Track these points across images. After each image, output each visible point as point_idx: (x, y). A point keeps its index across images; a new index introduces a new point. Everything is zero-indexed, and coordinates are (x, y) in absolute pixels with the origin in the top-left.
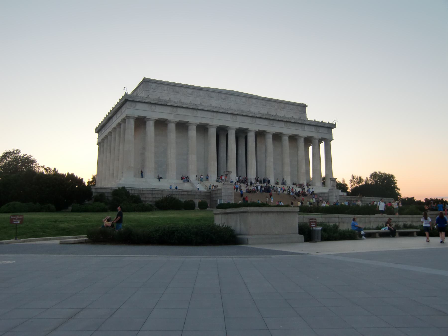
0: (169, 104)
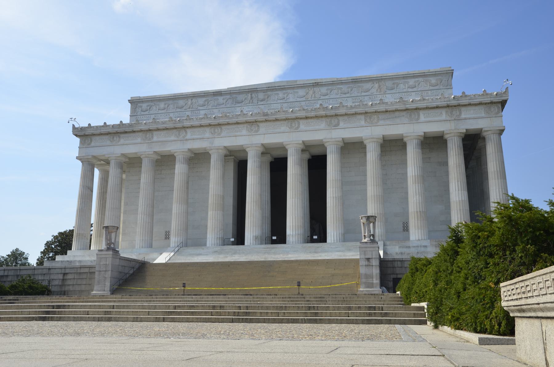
0: (136, 129)
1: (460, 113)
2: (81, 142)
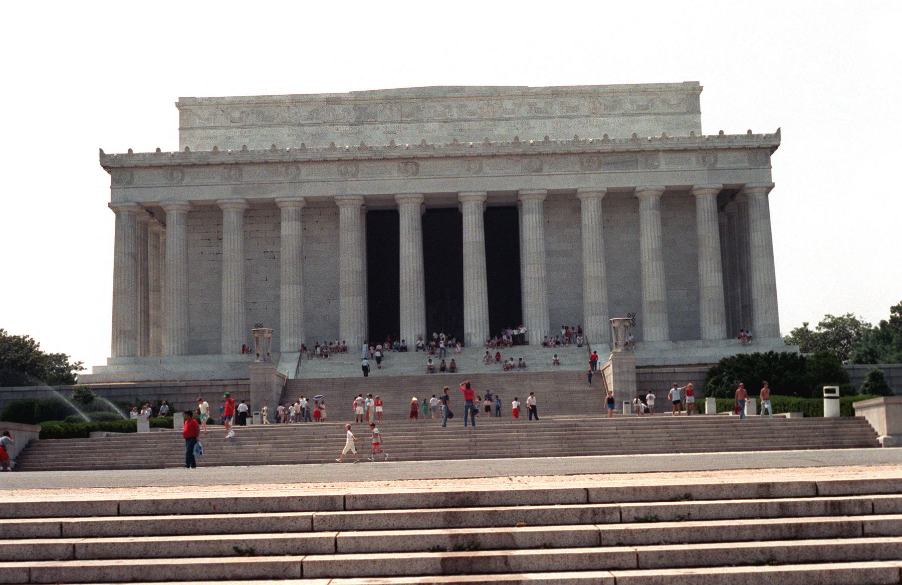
1: (716, 160)
2: (113, 180)
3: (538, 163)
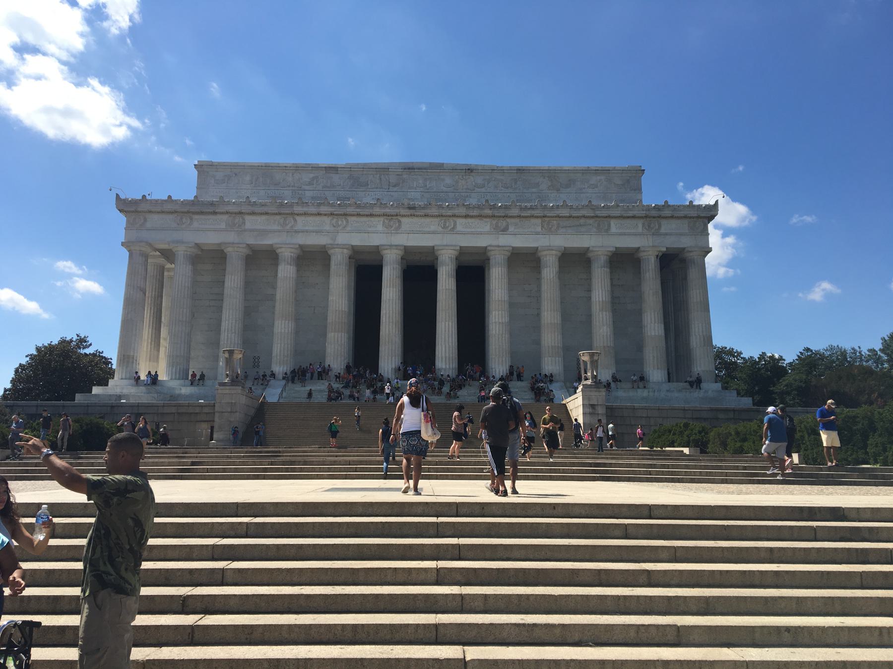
2: (128, 221)
3: (504, 224)
